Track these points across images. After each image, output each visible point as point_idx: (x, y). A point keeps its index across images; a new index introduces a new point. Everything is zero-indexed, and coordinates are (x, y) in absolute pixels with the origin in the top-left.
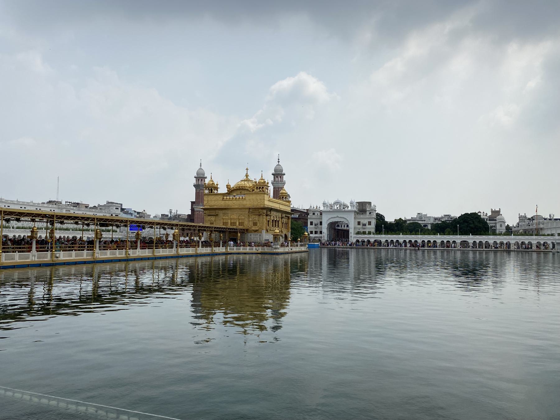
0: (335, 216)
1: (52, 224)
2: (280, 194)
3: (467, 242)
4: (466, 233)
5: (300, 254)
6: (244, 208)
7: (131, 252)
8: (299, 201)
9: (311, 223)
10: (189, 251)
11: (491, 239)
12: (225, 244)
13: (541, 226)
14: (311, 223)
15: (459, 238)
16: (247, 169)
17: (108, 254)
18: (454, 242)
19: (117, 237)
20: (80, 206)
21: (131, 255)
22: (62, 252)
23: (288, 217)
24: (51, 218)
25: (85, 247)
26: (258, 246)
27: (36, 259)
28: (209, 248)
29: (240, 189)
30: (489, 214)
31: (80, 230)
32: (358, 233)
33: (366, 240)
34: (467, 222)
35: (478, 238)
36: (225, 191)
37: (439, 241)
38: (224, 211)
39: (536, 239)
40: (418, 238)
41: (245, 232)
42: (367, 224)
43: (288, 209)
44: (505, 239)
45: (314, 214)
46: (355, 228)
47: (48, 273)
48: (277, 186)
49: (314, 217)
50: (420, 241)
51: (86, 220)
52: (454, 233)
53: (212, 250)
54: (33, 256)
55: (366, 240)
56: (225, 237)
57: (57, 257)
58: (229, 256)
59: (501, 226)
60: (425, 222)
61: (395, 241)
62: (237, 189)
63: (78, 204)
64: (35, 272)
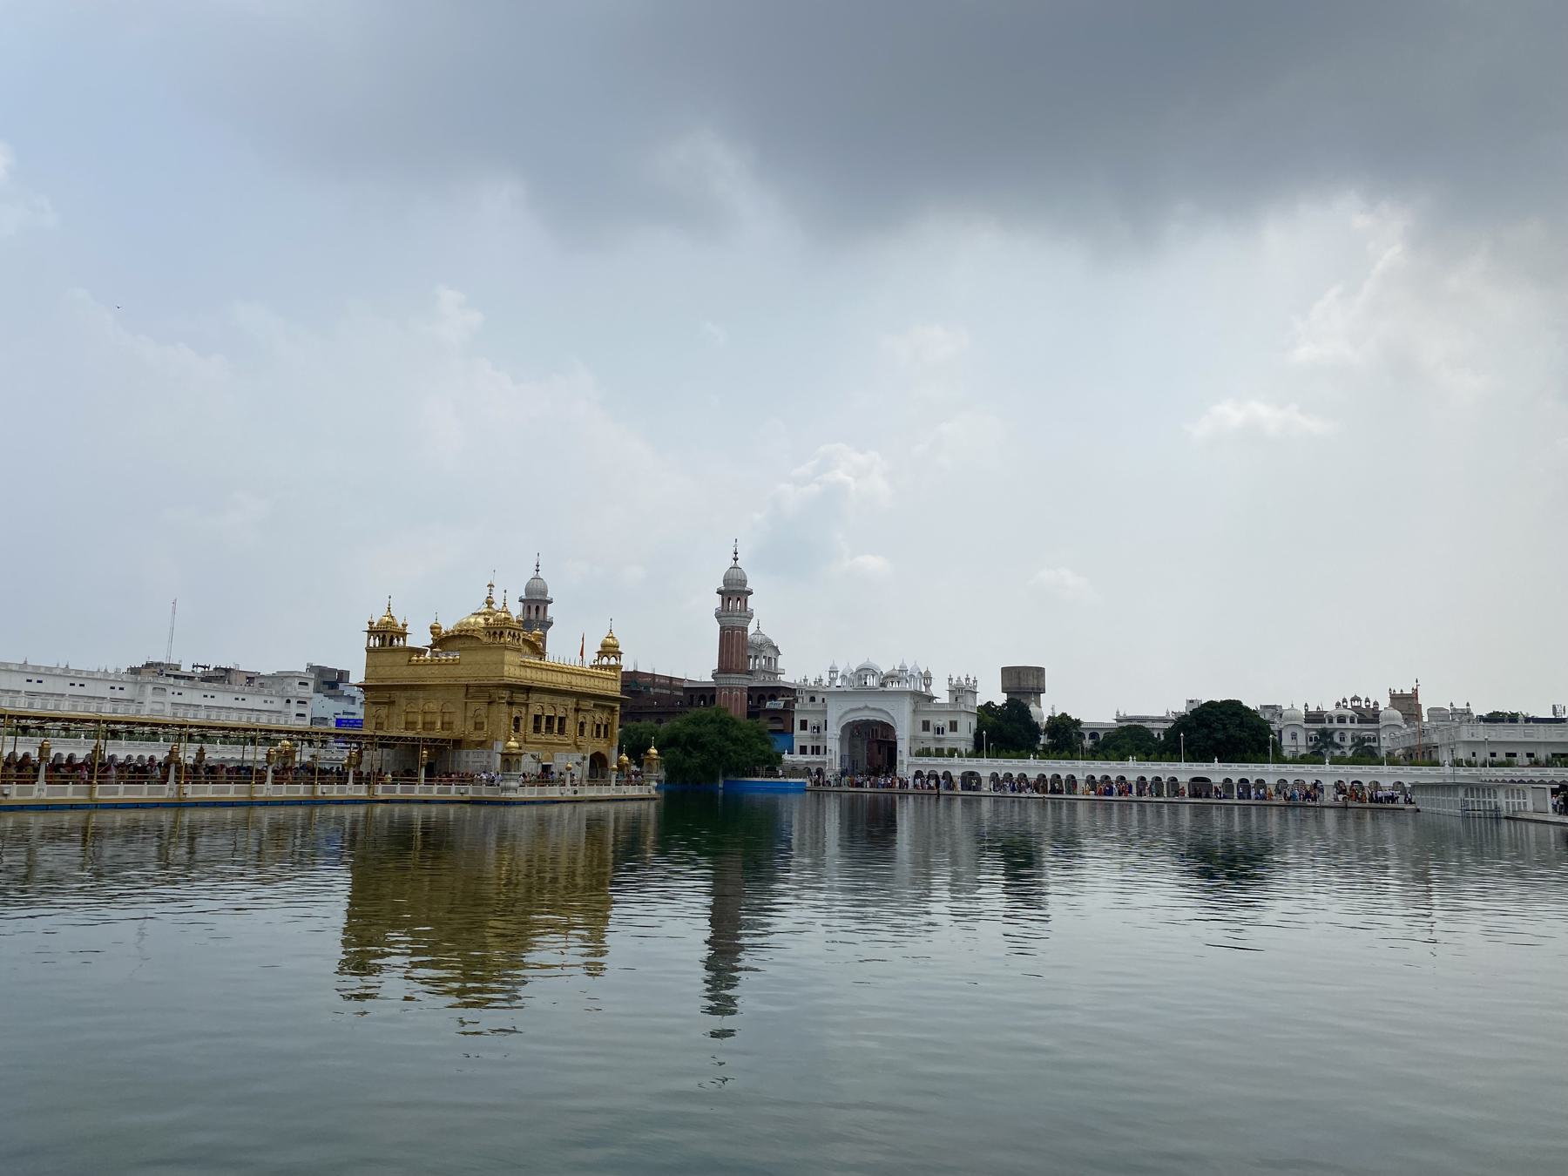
0: (861, 705)
3: (1225, 783)
9: (804, 725)
11: (1268, 773)
14: (804, 725)
15: (1184, 771)
16: (491, 585)
20: (233, 677)
23: (612, 709)
29: (460, 636)
32: (925, 753)
33: (940, 773)
34: (1208, 726)
35: (1236, 771)
38: (408, 694)
40: (1077, 769)
42: (947, 728)
43: (614, 688)
44: (1308, 774)
46: (914, 739)
48: (729, 622)
49: (810, 707)
63: (227, 670)
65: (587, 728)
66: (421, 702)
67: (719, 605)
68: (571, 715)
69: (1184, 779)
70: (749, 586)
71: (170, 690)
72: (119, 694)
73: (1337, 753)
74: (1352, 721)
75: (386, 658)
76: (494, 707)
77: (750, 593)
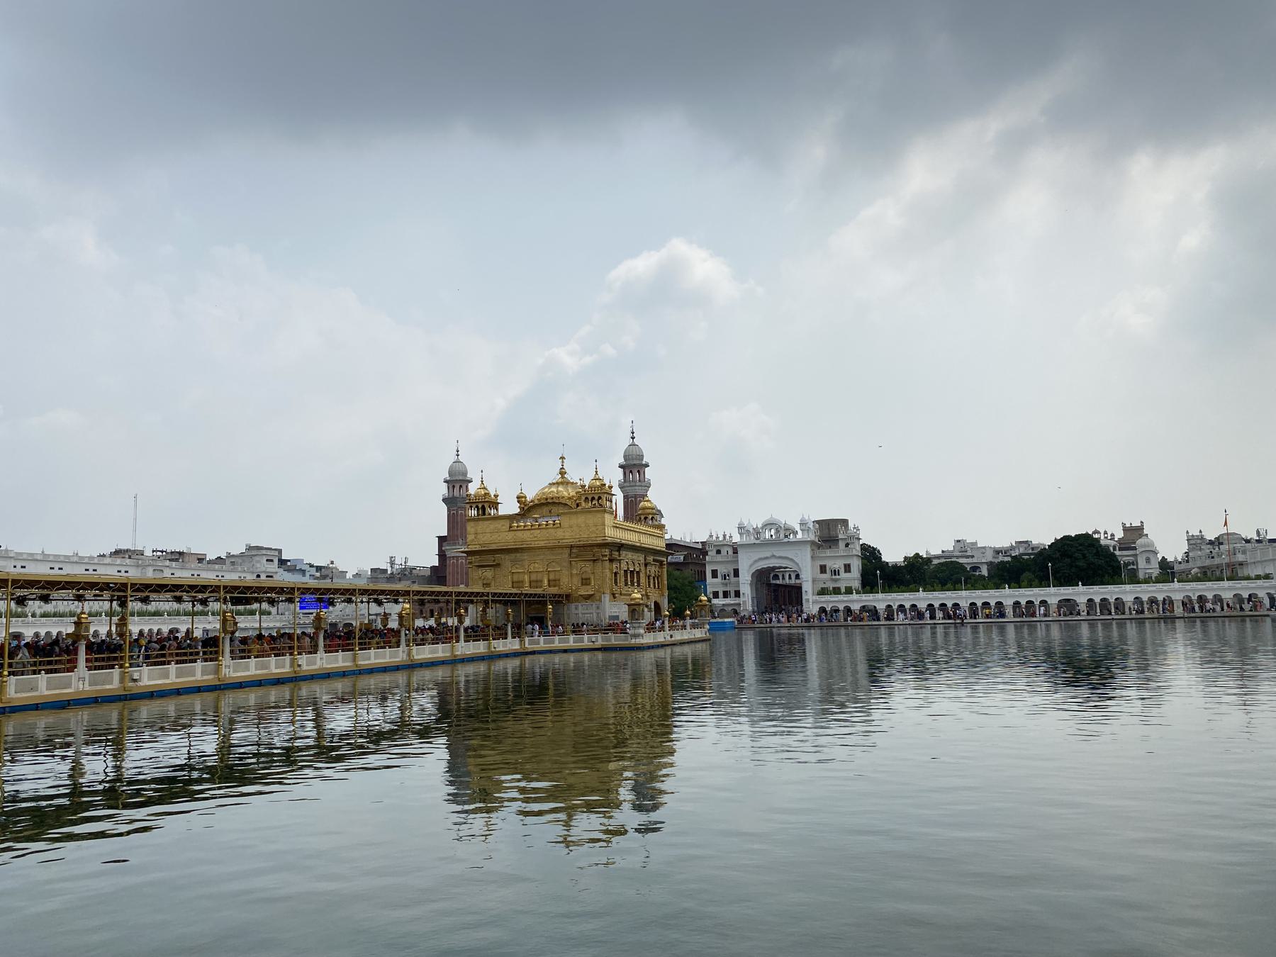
0: (768, 554)
1: (123, 604)
2: (639, 511)
3: (1073, 602)
5: (692, 646)
6: (560, 547)
7: (303, 660)
8: (683, 526)
10: (435, 651)
11: (1127, 593)
12: (518, 632)
13: (1240, 557)
15: (1054, 594)
16: (562, 458)
17: (252, 668)
18: (1044, 603)
19: (271, 625)
20: (186, 559)
21: (305, 667)
22: (145, 669)
23: (661, 563)
24: (120, 592)
25: (197, 653)
26: (595, 631)
27: (87, 688)
28: (481, 643)
30: (1119, 534)
31: (186, 614)
32: (823, 592)
34: (1070, 557)
35: (1098, 592)
36: (515, 509)
37: (1008, 603)
39: (1230, 589)
40: (961, 598)
41: (562, 600)
42: (842, 570)
43: (660, 545)
44: (1160, 591)
45: (719, 552)
46: (814, 581)
47: (115, 715)
48: (631, 491)
49: (719, 558)
50: (964, 604)
51: (199, 593)
52: (1043, 581)
53: (489, 647)
54: (81, 680)
55: (841, 607)
57: (135, 680)
58: (528, 659)
59: (1148, 560)
60: (975, 560)
61: (907, 606)
62: (542, 504)
63: (181, 554)
64: (85, 717)
66: (526, 563)
69: (1053, 601)
70: (645, 460)
76: (599, 564)
77: (647, 465)
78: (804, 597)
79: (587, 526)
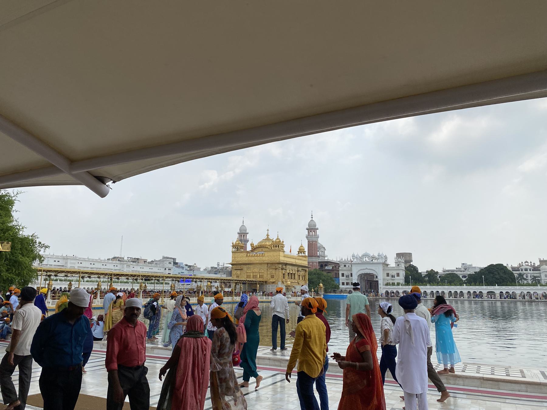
0: (365, 268)
2: (314, 247)
4: (492, 284)
8: (332, 255)
9: (343, 275)
11: (517, 290)
14: (343, 275)
15: (485, 289)
20: (140, 261)
23: (306, 271)
24: (111, 276)
32: (387, 284)
33: (395, 292)
34: (493, 273)
35: (505, 289)
37: (465, 292)
38: (247, 266)
41: (263, 283)
42: (396, 276)
45: (345, 266)
46: (384, 279)
48: (311, 239)
49: (345, 268)
52: (481, 284)
56: (244, 288)
60: (465, 273)
63: (138, 259)
65: (301, 277)
67: (307, 233)
68: (296, 272)
69: (485, 292)
71: (132, 266)
72: (116, 268)
73: (525, 282)
74: (530, 270)
75: (237, 254)
77: (317, 229)
78: (379, 286)
79: (274, 256)
